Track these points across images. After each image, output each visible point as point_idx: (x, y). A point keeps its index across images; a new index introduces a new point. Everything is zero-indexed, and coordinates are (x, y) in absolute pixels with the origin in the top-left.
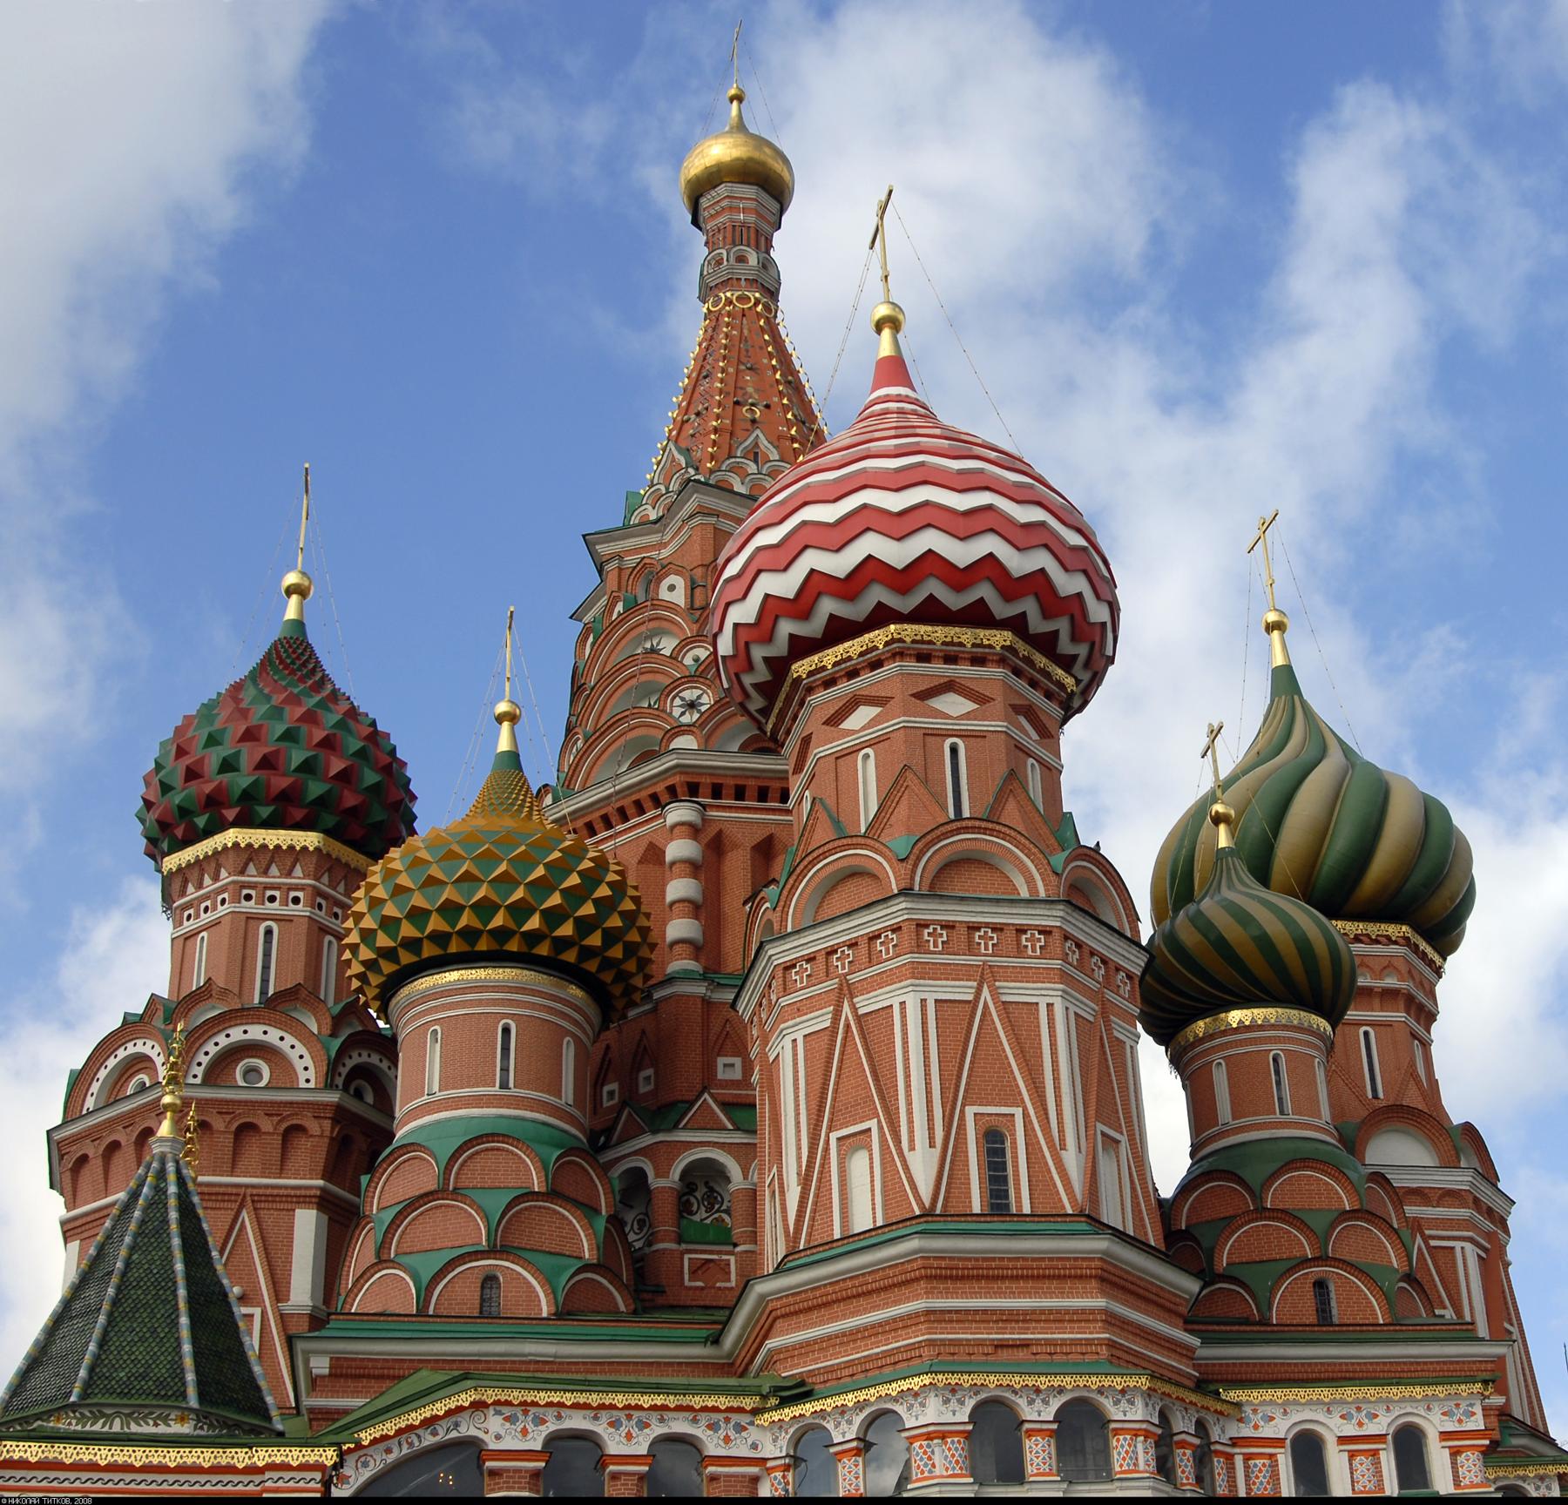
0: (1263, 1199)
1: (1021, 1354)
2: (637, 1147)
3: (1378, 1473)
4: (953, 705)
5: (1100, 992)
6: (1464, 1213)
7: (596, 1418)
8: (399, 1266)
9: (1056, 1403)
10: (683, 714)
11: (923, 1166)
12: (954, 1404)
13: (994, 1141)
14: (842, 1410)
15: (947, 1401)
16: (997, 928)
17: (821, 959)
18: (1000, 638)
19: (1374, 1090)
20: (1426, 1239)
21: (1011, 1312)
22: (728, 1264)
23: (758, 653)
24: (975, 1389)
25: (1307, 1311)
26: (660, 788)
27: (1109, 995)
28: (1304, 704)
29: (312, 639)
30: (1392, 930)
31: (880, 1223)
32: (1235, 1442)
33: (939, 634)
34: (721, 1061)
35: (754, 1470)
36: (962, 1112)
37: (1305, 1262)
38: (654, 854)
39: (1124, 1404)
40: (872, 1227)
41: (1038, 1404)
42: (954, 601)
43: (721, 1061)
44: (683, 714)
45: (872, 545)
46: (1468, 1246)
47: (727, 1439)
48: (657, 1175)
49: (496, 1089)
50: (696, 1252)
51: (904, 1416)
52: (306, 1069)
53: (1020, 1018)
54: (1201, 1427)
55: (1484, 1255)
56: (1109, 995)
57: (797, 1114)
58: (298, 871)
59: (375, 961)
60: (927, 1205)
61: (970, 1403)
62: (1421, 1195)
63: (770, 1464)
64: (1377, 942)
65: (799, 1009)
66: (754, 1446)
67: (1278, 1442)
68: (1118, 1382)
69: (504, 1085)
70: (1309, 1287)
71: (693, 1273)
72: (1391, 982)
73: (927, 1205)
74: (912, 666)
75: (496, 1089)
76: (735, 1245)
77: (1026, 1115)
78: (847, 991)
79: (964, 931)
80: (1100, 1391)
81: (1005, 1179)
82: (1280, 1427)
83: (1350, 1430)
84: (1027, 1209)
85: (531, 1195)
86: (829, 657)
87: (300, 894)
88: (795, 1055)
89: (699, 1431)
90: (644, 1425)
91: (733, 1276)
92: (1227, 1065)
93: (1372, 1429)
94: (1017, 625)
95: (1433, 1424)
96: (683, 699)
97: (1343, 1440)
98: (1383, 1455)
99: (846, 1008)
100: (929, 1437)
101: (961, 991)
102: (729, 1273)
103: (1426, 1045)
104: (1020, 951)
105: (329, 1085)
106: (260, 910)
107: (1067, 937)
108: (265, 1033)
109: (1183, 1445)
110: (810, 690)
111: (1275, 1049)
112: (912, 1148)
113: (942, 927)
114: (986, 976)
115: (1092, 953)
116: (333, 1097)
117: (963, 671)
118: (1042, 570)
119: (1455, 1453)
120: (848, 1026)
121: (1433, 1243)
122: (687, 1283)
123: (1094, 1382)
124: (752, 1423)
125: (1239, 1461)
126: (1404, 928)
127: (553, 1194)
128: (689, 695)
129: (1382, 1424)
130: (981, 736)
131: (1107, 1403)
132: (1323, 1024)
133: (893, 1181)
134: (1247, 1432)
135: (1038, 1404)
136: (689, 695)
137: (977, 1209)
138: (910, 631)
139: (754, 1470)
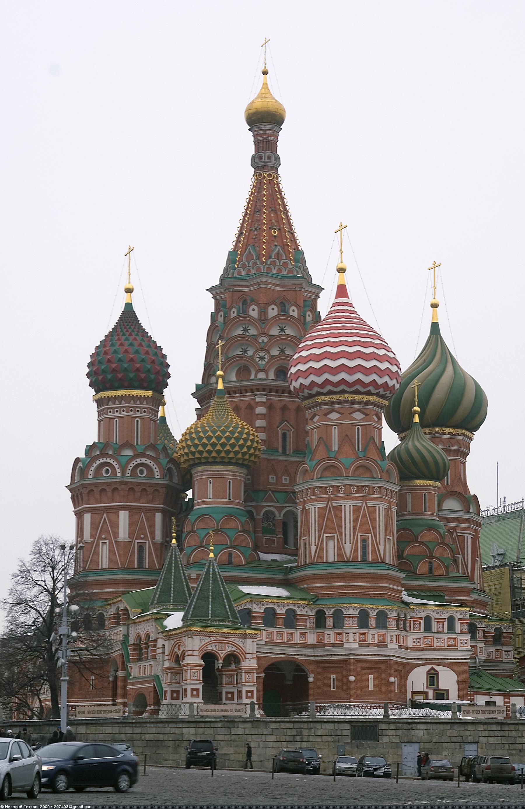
0: (418, 538)
1: (368, 596)
2: (251, 505)
3: (443, 627)
4: (358, 416)
5: (389, 500)
6: (468, 525)
7: (274, 605)
8: (206, 548)
9: (377, 611)
10: (259, 361)
11: (348, 548)
12: (355, 610)
13: (364, 541)
14: (329, 608)
15: (354, 609)
16: (368, 487)
17: (324, 488)
18: (373, 399)
19: (447, 482)
20: (457, 533)
21: (366, 586)
22: (274, 540)
23: (306, 391)
24: (360, 608)
25: (426, 571)
26: (254, 388)
27: (391, 500)
28: (441, 337)
29: (136, 309)
30: (459, 431)
31: (336, 560)
32: (411, 618)
33: (357, 398)
34: (270, 477)
35: (307, 617)
36: (357, 535)
37: (428, 557)
38: (251, 408)
39: (391, 612)
40: (333, 561)
41: (373, 611)
42: (362, 390)
43: (270, 477)
44: (259, 361)
45: (343, 375)
46: (469, 536)
47: (301, 610)
48: (257, 515)
49: (227, 500)
50: (266, 536)
51: (344, 611)
52: (157, 474)
53: (372, 511)
54: (405, 615)
55: (473, 537)
56: (391, 500)
57: (315, 527)
58: (145, 403)
59: (188, 453)
60: (348, 557)
61: (359, 610)
62: (458, 520)
63: (310, 616)
64: (454, 435)
65: (317, 500)
66: (307, 612)
67: (421, 618)
68: (391, 608)
69: (230, 499)
70: (427, 564)
71: (266, 542)
72: (456, 447)
73: (348, 557)
74: (349, 405)
75: (227, 500)
76: (277, 535)
77: (372, 536)
78: (329, 499)
79: (360, 487)
80: (386, 609)
81: (366, 552)
82: (423, 615)
83: (438, 616)
84: (370, 560)
85: (241, 532)
86: (328, 398)
87: (146, 410)
88: (315, 512)
89: (295, 608)
90: (284, 606)
91: (276, 544)
92: (411, 495)
93: (443, 617)
94: (377, 395)
95: (457, 616)
96: (259, 355)
97: (435, 619)
98: (444, 623)
99: (330, 503)
100: (350, 617)
101: (358, 503)
102: (275, 543)
103: (464, 464)
104: (374, 494)
105: (163, 478)
106: (135, 415)
107: (384, 488)
108: (146, 461)
109: (401, 619)
110: (320, 404)
111: (425, 492)
112: (345, 544)
113: (356, 486)
114: (365, 499)
115: (389, 489)
116: (167, 482)
117: (362, 407)
118: (386, 382)
119: (461, 624)
120: (330, 508)
121: (459, 534)
122: (264, 545)
123: (385, 607)
124: (306, 607)
125: (412, 622)
126: (463, 431)
127: (244, 531)
128: (262, 354)
129: (446, 616)
130: (365, 425)
131: (387, 611)
132: (439, 484)
133: (340, 551)
134: (415, 615)
135: (373, 611)
136: (262, 354)
137: (359, 560)
138: (350, 397)
139: (307, 617)
